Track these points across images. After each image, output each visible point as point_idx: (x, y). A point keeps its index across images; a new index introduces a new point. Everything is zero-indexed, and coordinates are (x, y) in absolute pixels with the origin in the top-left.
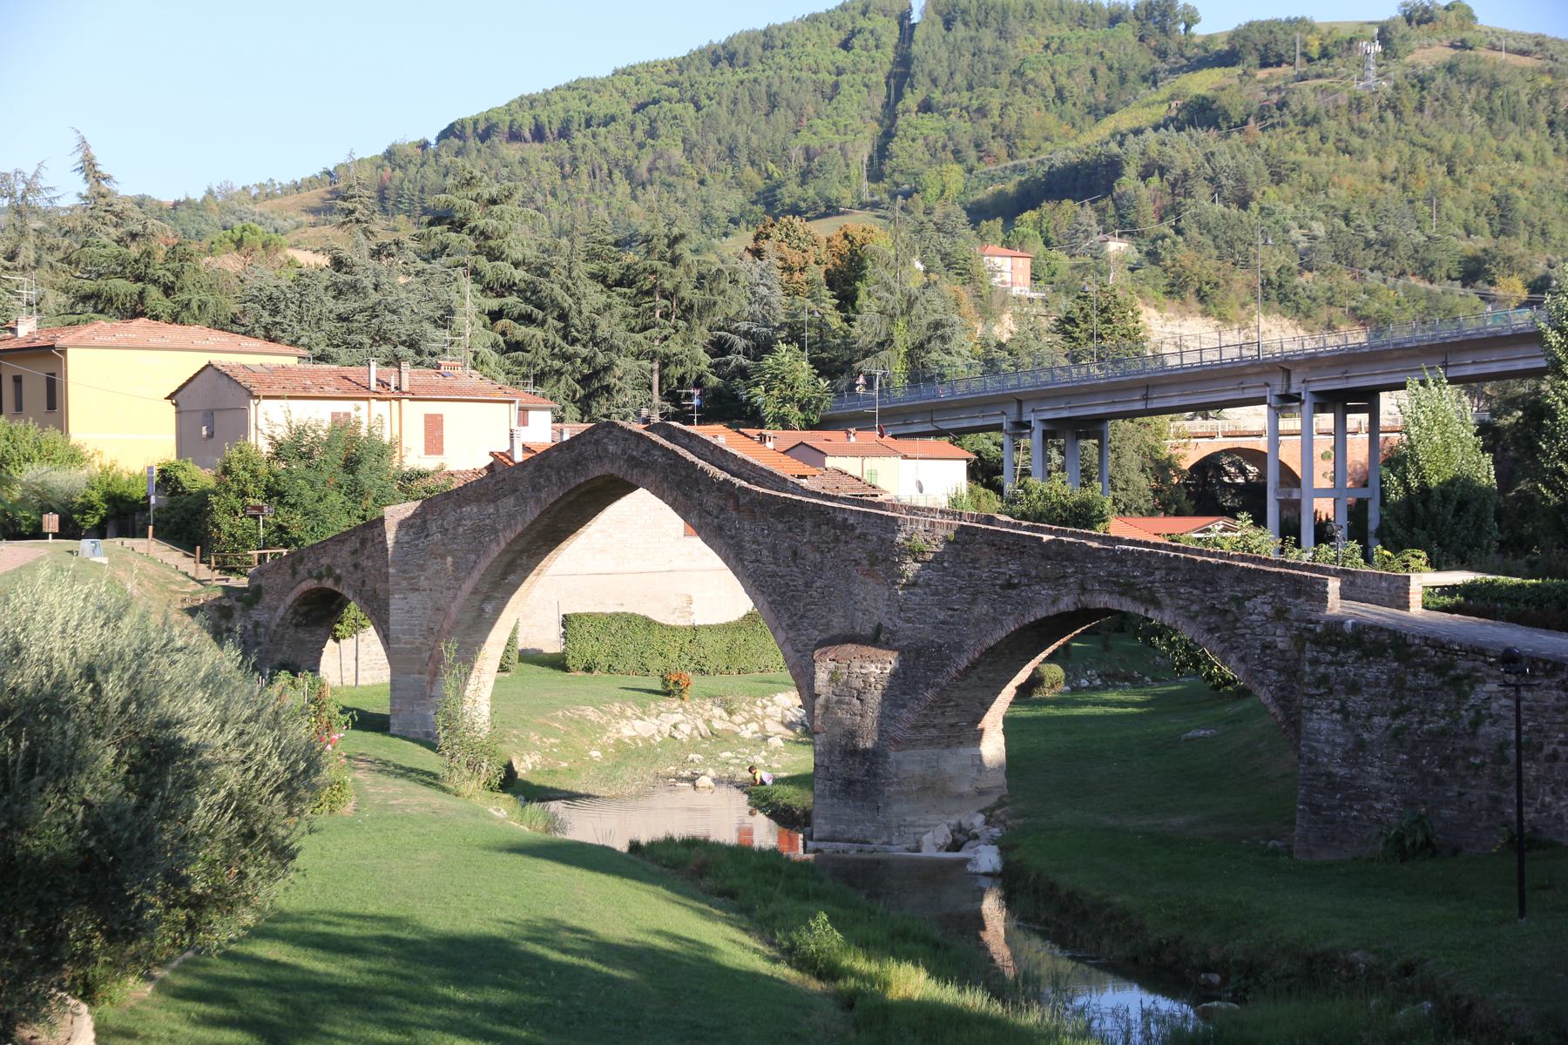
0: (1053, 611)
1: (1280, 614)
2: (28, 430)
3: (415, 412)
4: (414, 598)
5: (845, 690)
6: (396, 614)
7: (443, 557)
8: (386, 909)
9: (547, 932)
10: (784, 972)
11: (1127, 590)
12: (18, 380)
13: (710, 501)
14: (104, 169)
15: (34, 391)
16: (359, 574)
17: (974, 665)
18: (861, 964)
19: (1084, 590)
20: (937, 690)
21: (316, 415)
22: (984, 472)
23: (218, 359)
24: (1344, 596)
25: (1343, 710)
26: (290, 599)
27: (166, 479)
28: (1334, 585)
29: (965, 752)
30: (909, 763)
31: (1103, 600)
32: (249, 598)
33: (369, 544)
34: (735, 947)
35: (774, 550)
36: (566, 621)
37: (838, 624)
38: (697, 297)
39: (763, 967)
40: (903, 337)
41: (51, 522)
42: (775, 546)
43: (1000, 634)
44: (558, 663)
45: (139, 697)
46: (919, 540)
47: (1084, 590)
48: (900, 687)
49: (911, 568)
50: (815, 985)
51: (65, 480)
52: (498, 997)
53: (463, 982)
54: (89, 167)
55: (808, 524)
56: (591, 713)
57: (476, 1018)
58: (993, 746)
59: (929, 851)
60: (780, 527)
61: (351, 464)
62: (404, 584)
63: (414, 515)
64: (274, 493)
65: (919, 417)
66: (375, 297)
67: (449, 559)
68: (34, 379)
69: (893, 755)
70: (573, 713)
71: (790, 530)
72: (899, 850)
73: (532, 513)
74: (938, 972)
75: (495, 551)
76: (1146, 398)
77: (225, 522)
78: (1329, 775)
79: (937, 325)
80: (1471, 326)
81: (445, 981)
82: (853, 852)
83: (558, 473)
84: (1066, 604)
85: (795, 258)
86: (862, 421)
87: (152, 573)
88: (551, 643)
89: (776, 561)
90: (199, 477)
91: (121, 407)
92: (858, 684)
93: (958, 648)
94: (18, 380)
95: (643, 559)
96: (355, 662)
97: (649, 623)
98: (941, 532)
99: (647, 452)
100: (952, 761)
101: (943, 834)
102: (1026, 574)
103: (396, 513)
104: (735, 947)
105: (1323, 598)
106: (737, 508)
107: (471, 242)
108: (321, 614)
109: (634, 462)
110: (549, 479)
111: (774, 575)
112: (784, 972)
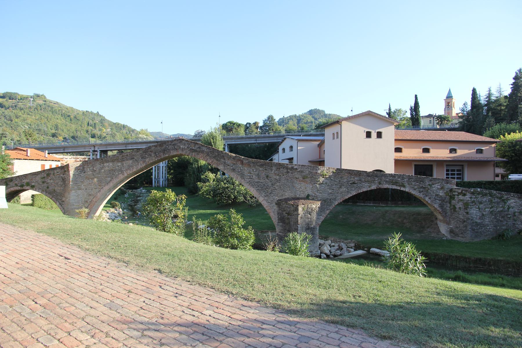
0: (369, 189)
4: (80, 192)
7: (93, 179)
11: (396, 183)
16: (45, 184)
19: (380, 183)
25: (479, 208)
33: (51, 175)
35: (258, 175)
42: (258, 174)
43: (350, 195)
46: (325, 172)
47: (380, 183)
49: (321, 179)
62: (76, 187)
63: (80, 166)
67: (96, 179)
71: (266, 170)
78: (476, 222)
80: (111, 142)
83: (155, 153)
89: (259, 178)
92: (310, 210)
93: (335, 199)
98: (331, 170)
99: (199, 148)
102: (360, 180)
110: (151, 155)
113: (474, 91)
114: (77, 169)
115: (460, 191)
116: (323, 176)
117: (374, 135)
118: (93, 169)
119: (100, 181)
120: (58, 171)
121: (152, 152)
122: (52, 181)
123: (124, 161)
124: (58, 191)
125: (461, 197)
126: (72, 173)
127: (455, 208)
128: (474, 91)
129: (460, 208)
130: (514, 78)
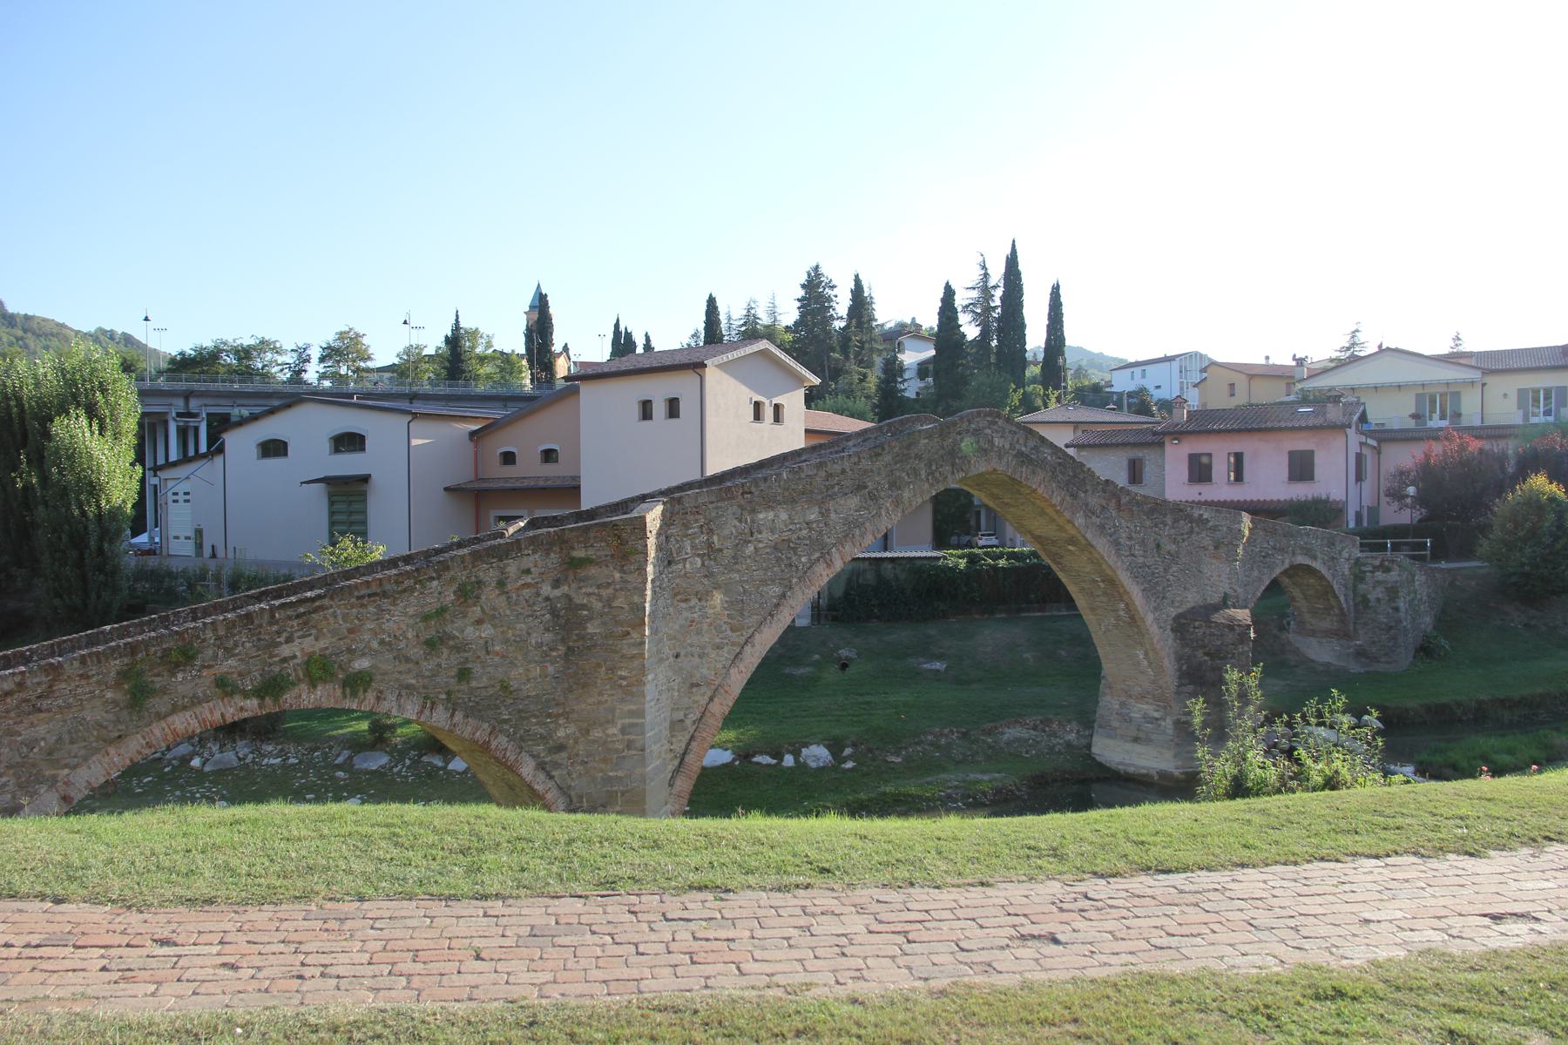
7: (703, 596)
13: (1094, 501)
16: (447, 659)
33: (490, 595)
55: (1169, 520)
60: (1148, 523)
67: (718, 598)
99: (1035, 448)
106: (1119, 507)
110: (916, 473)
111: (1145, 565)
113: (711, 302)
115: (1377, 563)
117: (659, 409)
118: (710, 545)
119: (737, 606)
120: (527, 562)
121: (918, 457)
122: (487, 631)
123: (832, 497)
124: (530, 689)
125: (1379, 575)
127: (1365, 600)
128: (711, 302)
129: (1378, 600)
130: (803, 286)
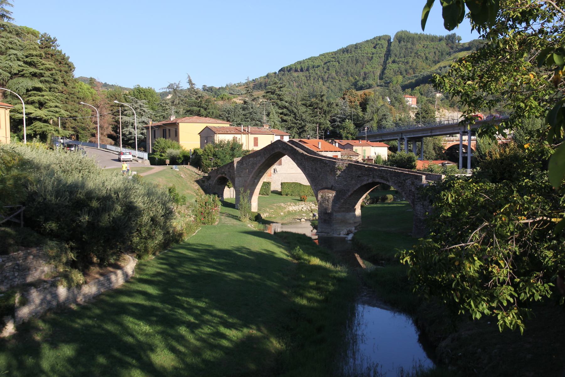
0: (367, 182)
1: (413, 183)
2: (169, 141)
3: (252, 137)
4: (240, 179)
5: (324, 199)
6: (236, 182)
8: (210, 244)
9: (239, 249)
10: (290, 258)
11: (382, 178)
12: (169, 130)
13: (299, 157)
14: (193, 82)
15: (173, 133)
17: (352, 194)
18: (306, 257)
19: (374, 178)
20: (345, 201)
21: (227, 138)
22: (392, 149)
23: (209, 125)
24: (426, 179)
25: (423, 205)
26: (216, 179)
27: (195, 152)
28: (424, 177)
29: (351, 214)
30: (339, 216)
31: (378, 180)
32: (208, 178)
34: (280, 252)
35: (312, 168)
36: (282, 184)
37: (324, 185)
38: (327, 109)
39: (285, 257)
40: (376, 118)
41: (168, 161)
44: (280, 193)
45: (126, 197)
46: (340, 166)
47: (374, 178)
48: (336, 199)
49: (339, 173)
50: (296, 261)
51: (174, 152)
52: (222, 261)
53: (215, 258)
54: (190, 82)
55: (319, 163)
56: (282, 205)
57: (215, 265)
58: (358, 212)
59: (342, 235)
61: (233, 149)
64: (215, 155)
65: (376, 138)
66: (251, 110)
68: (173, 130)
69: (335, 214)
70: (278, 205)
72: (335, 235)
73: (264, 160)
74: (322, 259)
75: (256, 168)
76: (431, 132)
77: (204, 161)
78: (420, 219)
79: (384, 115)
81: (213, 258)
82: (325, 235)
84: (370, 181)
85: (353, 99)
86: (363, 138)
87: (189, 172)
88: (279, 189)
90: (201, 152)
91: (189, 136)
92: (327, 198)
93: (348, 191)
94: (169, 130)
95: (287, 171)
96: (229, 193)
97: (300, 185)
98: (345, 165)
100: (348, 216)
101: (345, 231)
102: (362, 174)
103: (236, 160)
104: (280, 252)
105: (421, 180)
107: (276, 97)
108: (223, 182)
109: (284, 149)
112: (290, 258)
114: (238, 162)
116: (339, 169)
126: (235, 165)
